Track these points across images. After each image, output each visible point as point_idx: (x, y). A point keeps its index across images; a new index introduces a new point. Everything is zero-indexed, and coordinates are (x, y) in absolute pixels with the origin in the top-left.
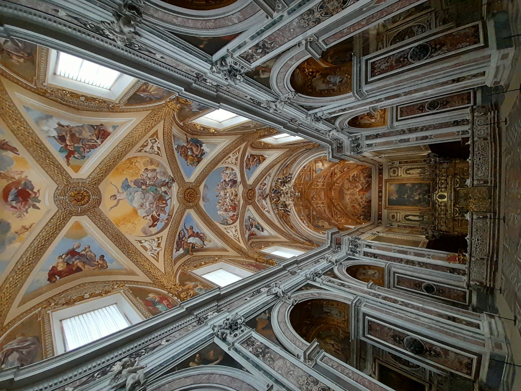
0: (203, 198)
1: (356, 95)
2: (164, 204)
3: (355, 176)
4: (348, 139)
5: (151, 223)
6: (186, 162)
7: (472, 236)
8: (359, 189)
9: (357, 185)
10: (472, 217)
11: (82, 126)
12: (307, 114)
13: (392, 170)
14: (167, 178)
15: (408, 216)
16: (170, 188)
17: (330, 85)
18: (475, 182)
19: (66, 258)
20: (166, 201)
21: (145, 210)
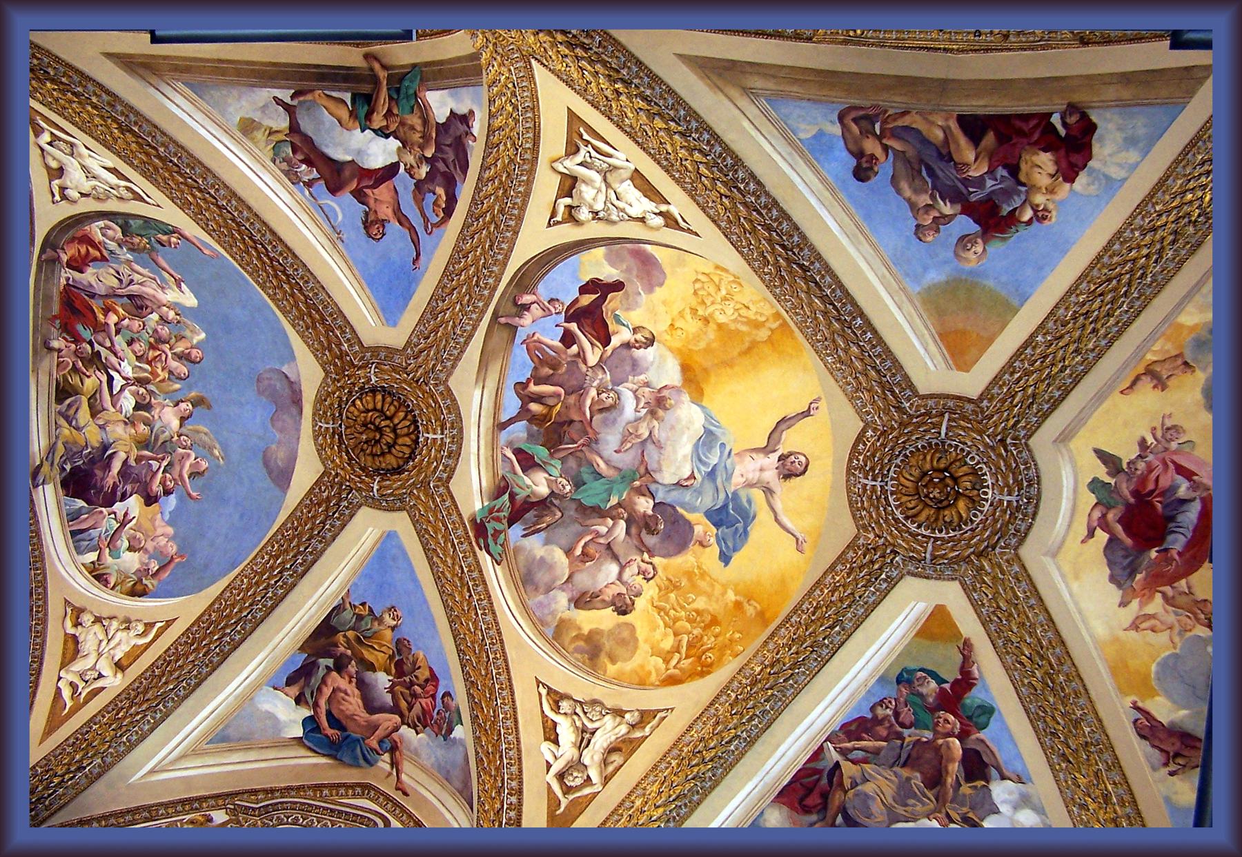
0: (297, 401)
2: (538, 399)
5: (613, 302)
6: (406, 632)
14: (517, 550)
16: (501, 488)
19: (1017, 202)
20: (524, 413)
21: (642, 377)
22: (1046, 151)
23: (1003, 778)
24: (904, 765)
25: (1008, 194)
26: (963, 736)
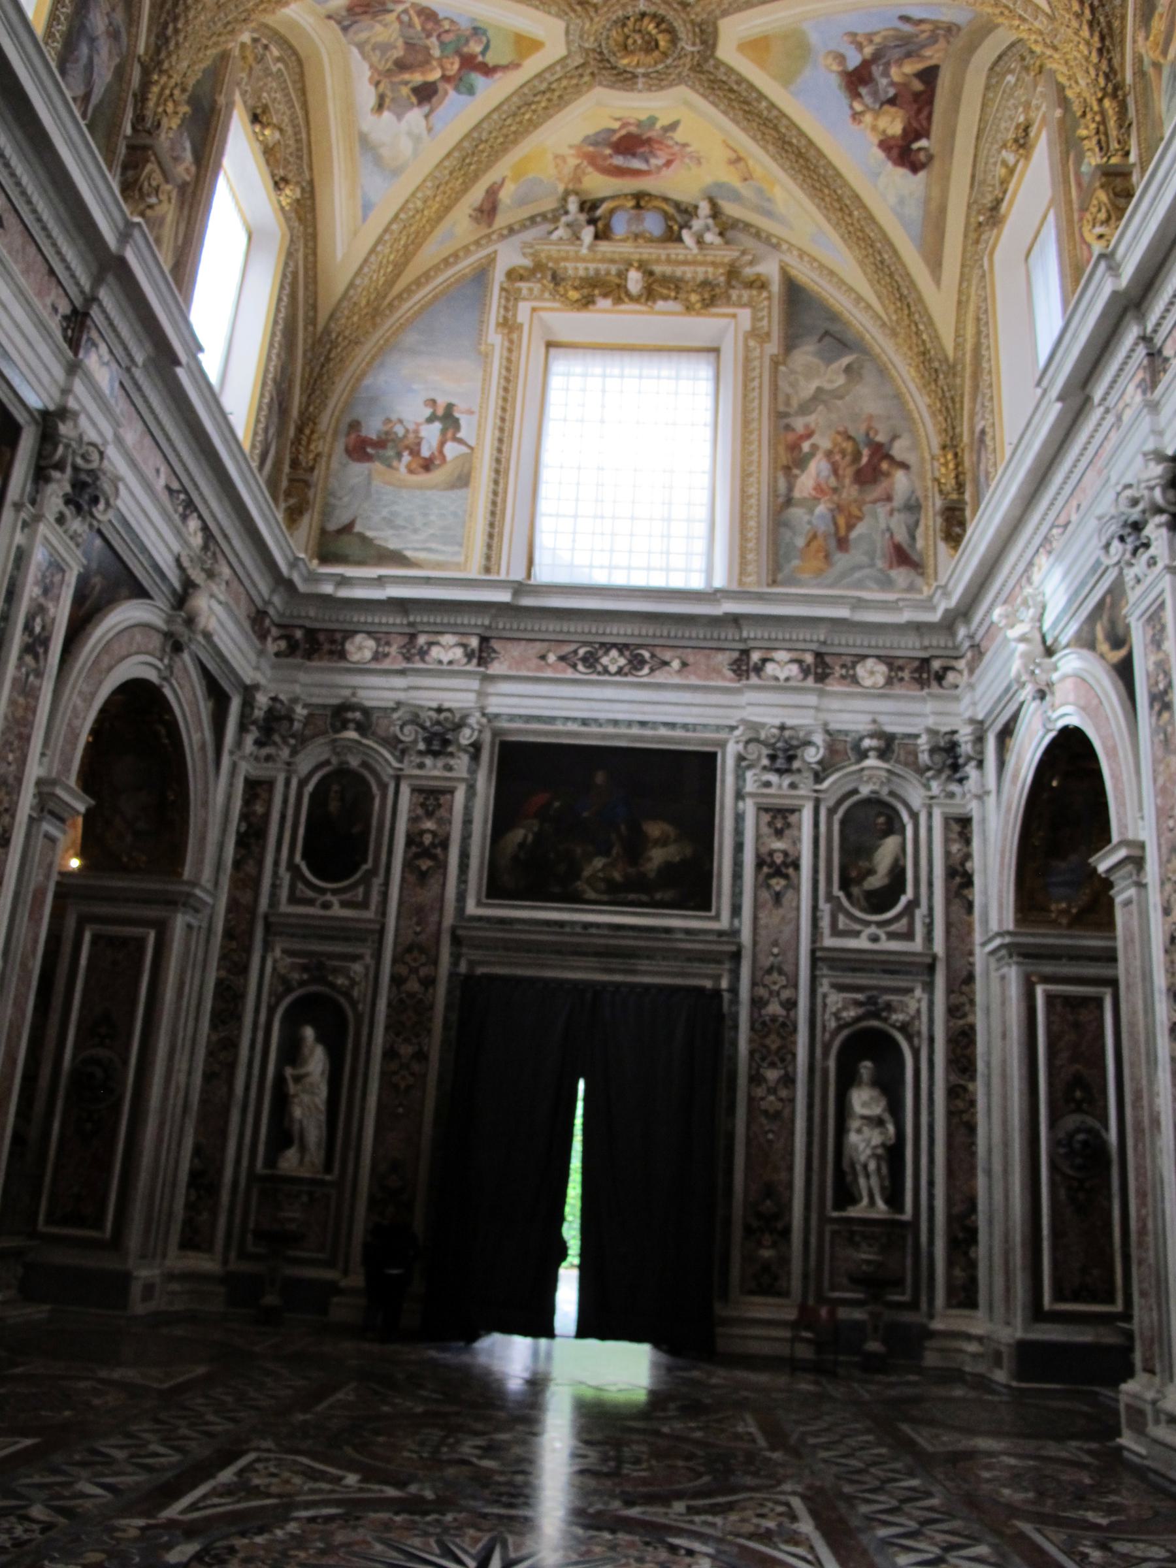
11: (360, 46)
19: (868, 100)
22: (905, 130)
23: (427, 116)
24: (406, 43)
25: (875, 94)
26: (445, 78)
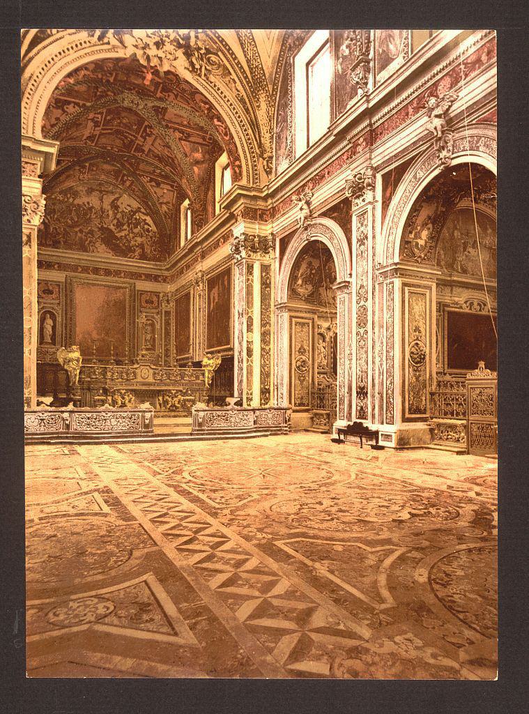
1: (394, 267)
3: (146, 227)
4: (272, 234)
7: (113, 412)
8: (116, 232)
9: (125, 227)
10: (147, 412)
12: (376, 170)
13: (155, 299)
15: (53, 317)
17: (419, 228)
18: (201, 414)
